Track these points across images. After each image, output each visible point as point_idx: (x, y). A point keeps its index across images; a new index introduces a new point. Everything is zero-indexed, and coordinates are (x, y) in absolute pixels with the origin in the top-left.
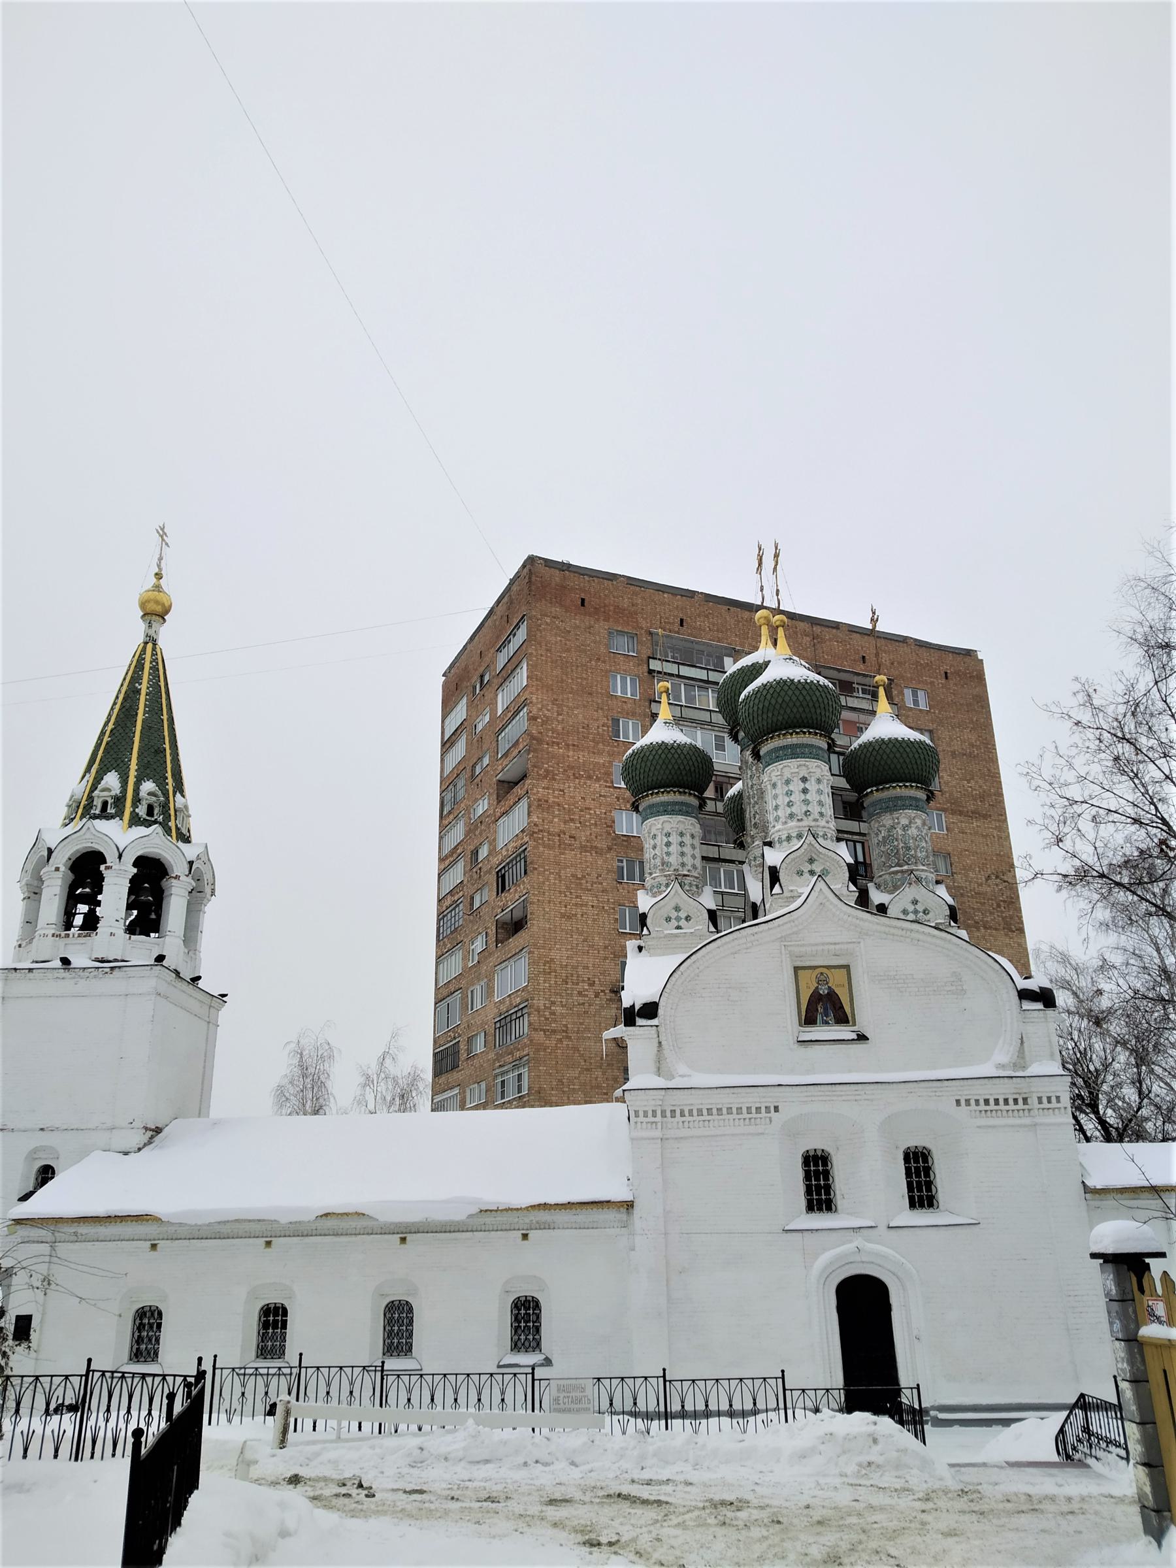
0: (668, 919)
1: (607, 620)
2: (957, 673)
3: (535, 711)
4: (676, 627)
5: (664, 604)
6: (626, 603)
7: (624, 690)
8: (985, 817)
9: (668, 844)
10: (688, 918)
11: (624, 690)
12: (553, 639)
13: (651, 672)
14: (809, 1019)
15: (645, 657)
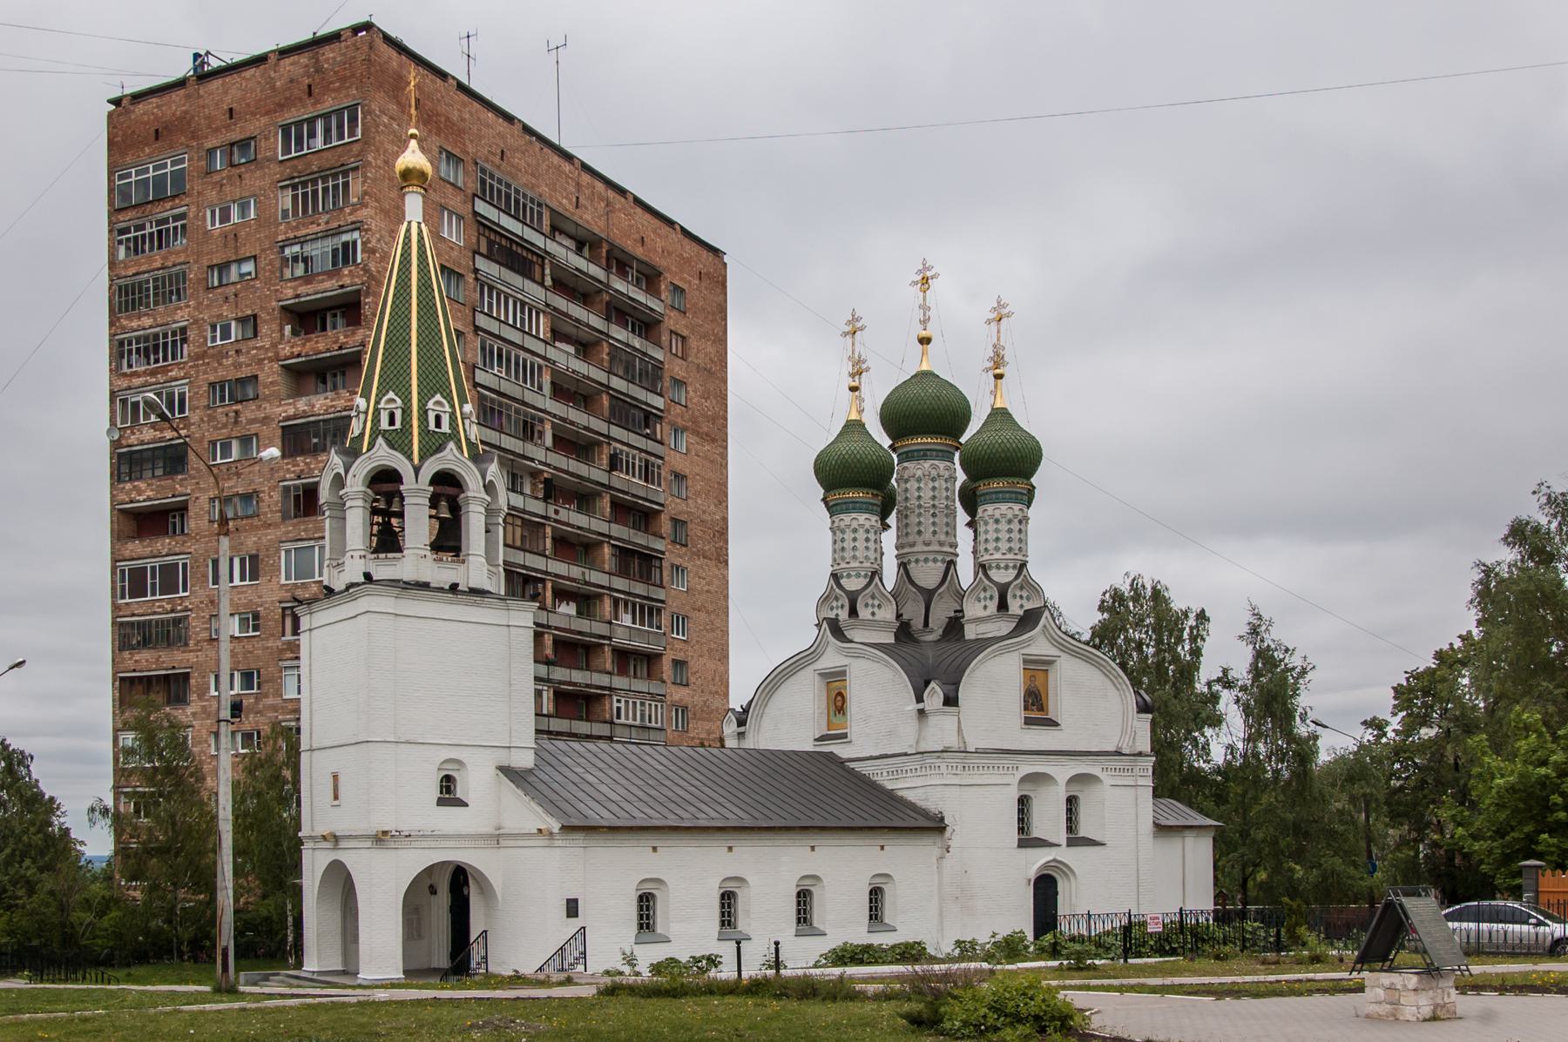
0: (867, 605)
1: (438, 135)
2: (708, 274)
3: (373, 243)
4: (497, 160)
5: (488, 126)
6: (455, 116)
7: (450, 233)
8: (714, 440)
9: (867, 540)
10: (879, 606)
11: (450, 233)
12: (389, 146)
13: (475, 214)
14: (1026, 709)
15: (470, 192)
